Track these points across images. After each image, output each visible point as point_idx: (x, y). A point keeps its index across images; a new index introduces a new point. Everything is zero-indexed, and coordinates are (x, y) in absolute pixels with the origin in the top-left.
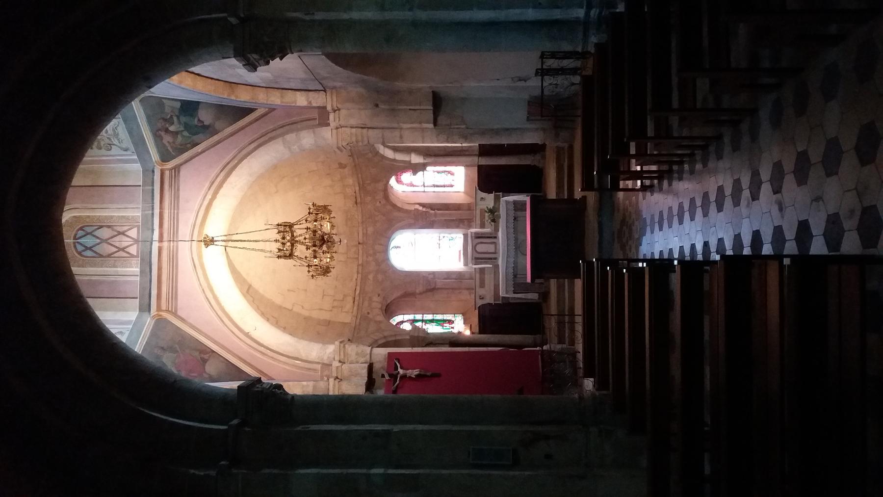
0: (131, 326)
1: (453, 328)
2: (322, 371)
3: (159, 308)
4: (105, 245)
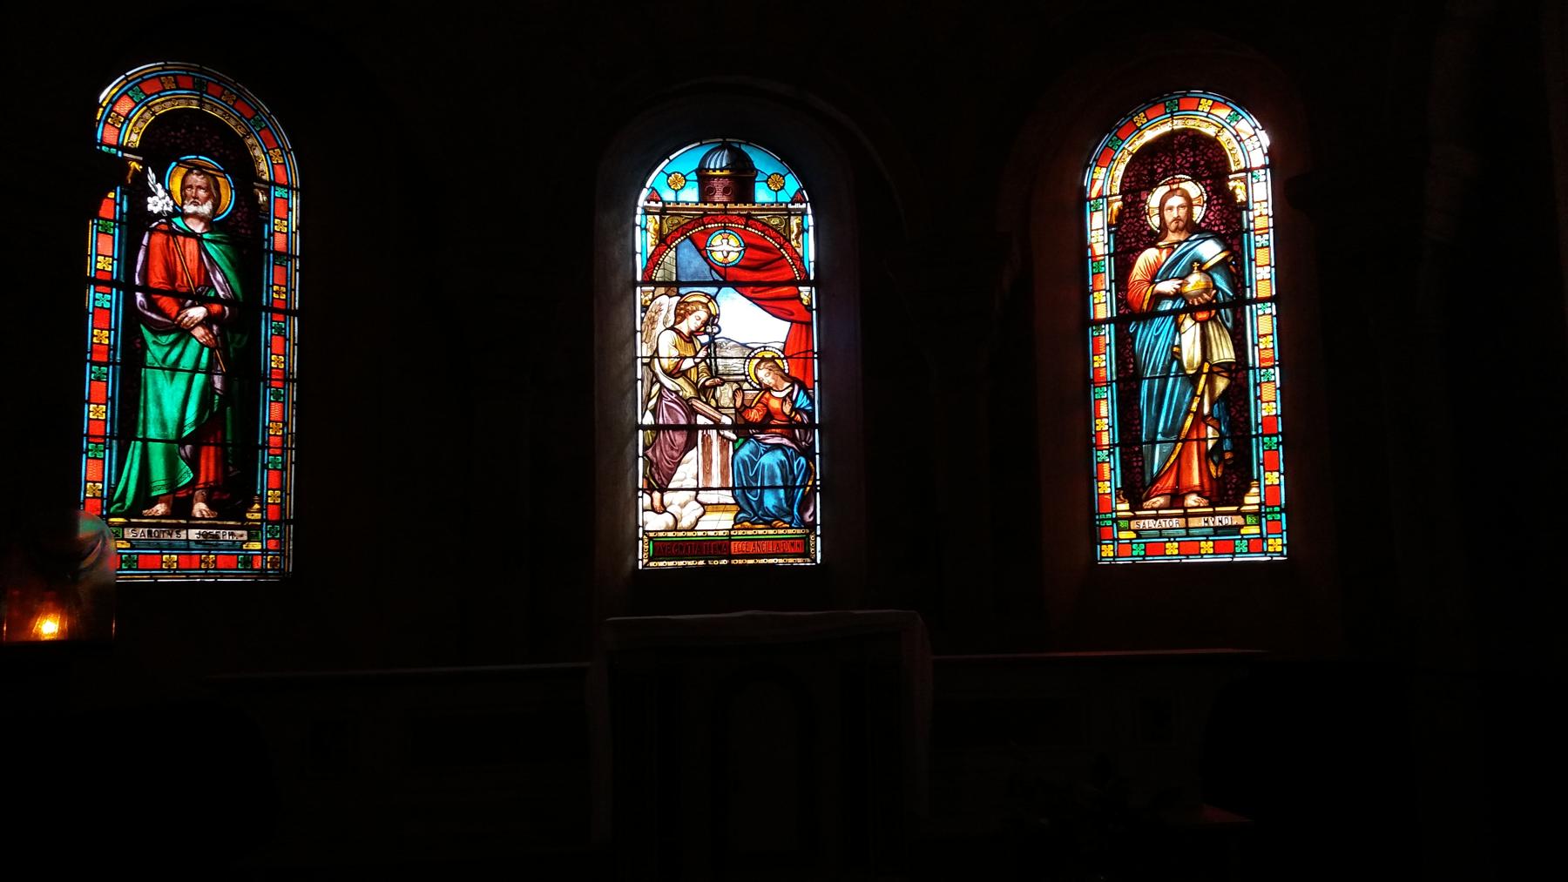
1: (180, 509)
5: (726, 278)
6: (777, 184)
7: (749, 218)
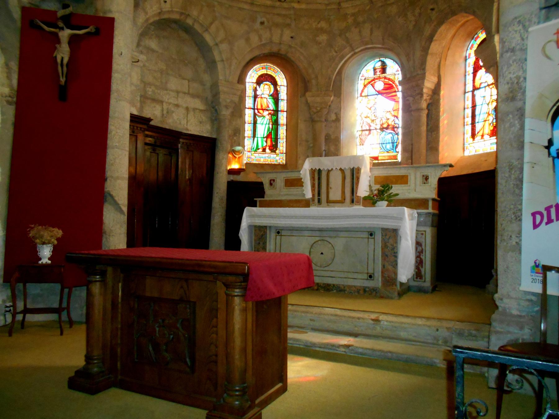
1: (264, 150)
7: (385, 78)
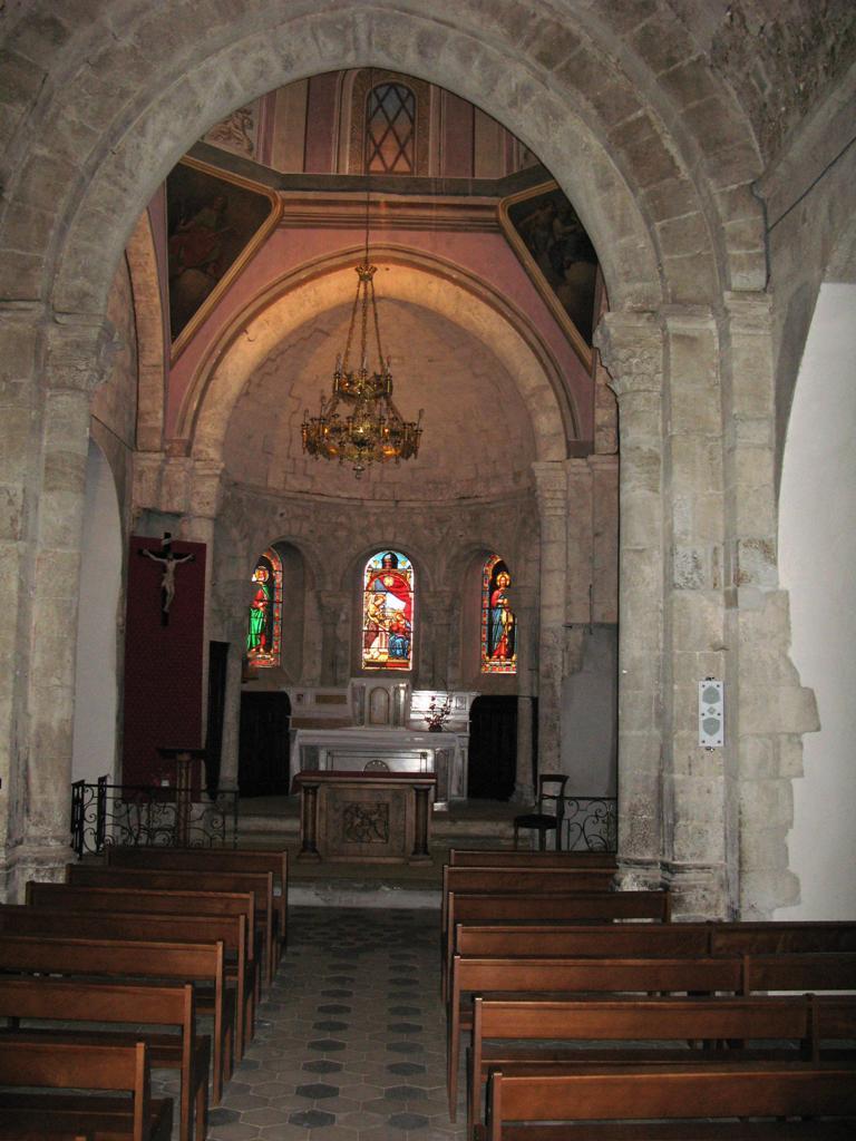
0: (260, 162)
1: (258, 650)
2: (178, 441)
3: (286, 202)
4: (385, 126)
5: (389, 590)
6: (404, 563)
